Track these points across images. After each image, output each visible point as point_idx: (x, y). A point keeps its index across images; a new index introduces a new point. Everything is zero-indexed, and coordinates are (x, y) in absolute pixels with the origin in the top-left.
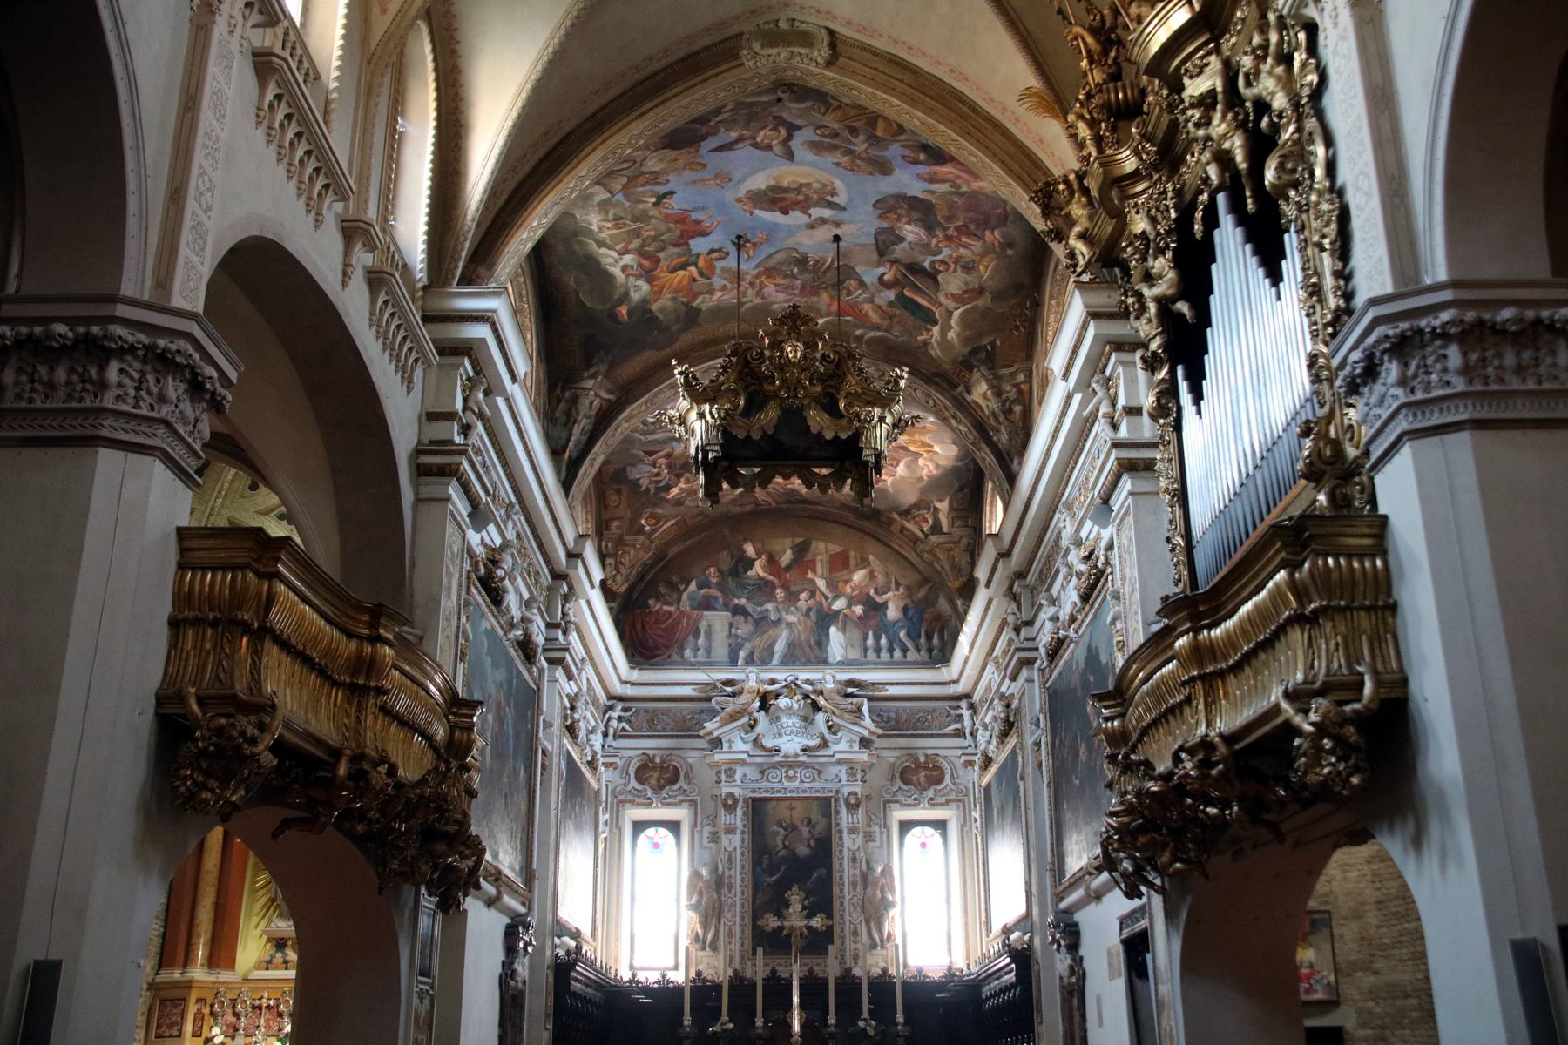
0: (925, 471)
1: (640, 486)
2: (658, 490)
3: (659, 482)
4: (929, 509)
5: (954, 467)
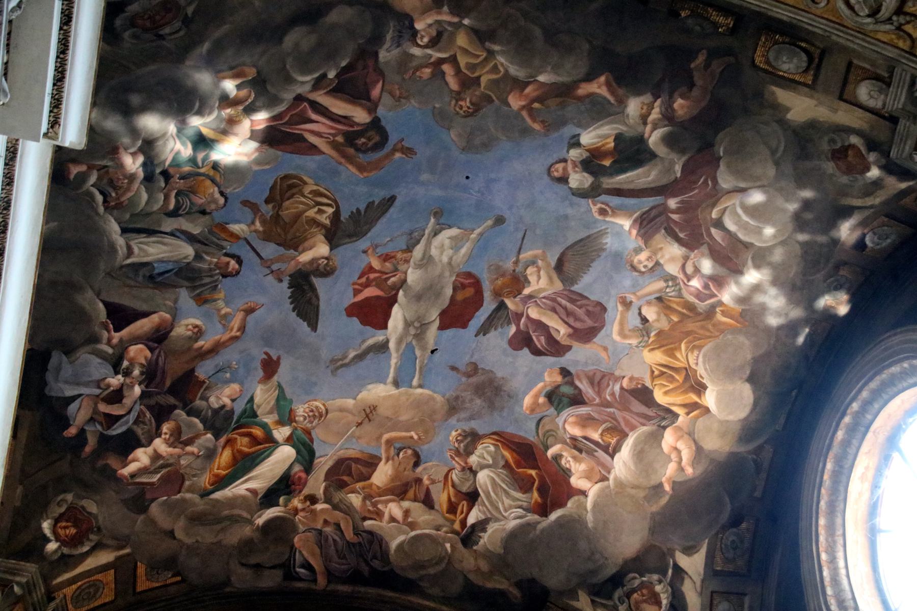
0: (671, 469)
1: (65, 423)
2: (104, 440)
3: (112, 420)
4: (664, 573)
5: (732, 455)
